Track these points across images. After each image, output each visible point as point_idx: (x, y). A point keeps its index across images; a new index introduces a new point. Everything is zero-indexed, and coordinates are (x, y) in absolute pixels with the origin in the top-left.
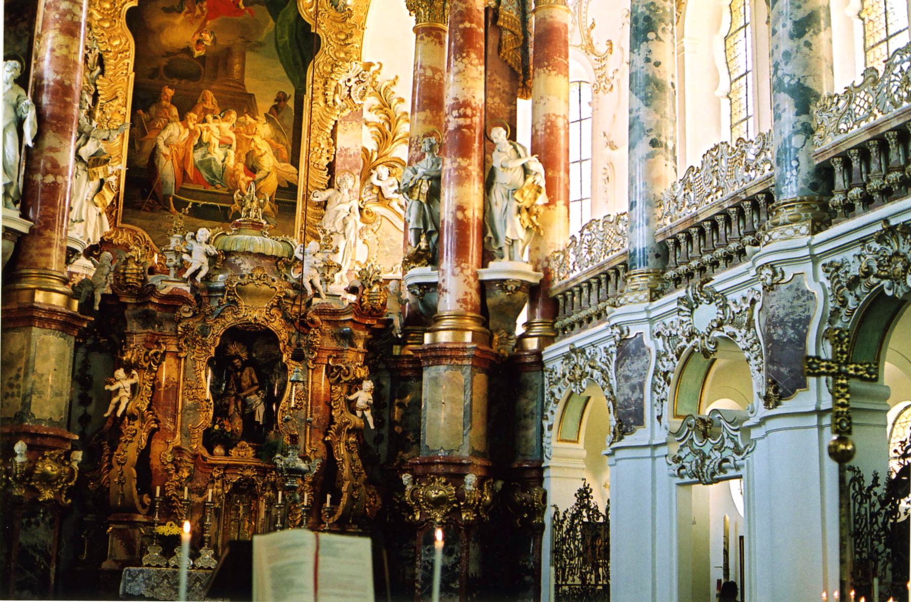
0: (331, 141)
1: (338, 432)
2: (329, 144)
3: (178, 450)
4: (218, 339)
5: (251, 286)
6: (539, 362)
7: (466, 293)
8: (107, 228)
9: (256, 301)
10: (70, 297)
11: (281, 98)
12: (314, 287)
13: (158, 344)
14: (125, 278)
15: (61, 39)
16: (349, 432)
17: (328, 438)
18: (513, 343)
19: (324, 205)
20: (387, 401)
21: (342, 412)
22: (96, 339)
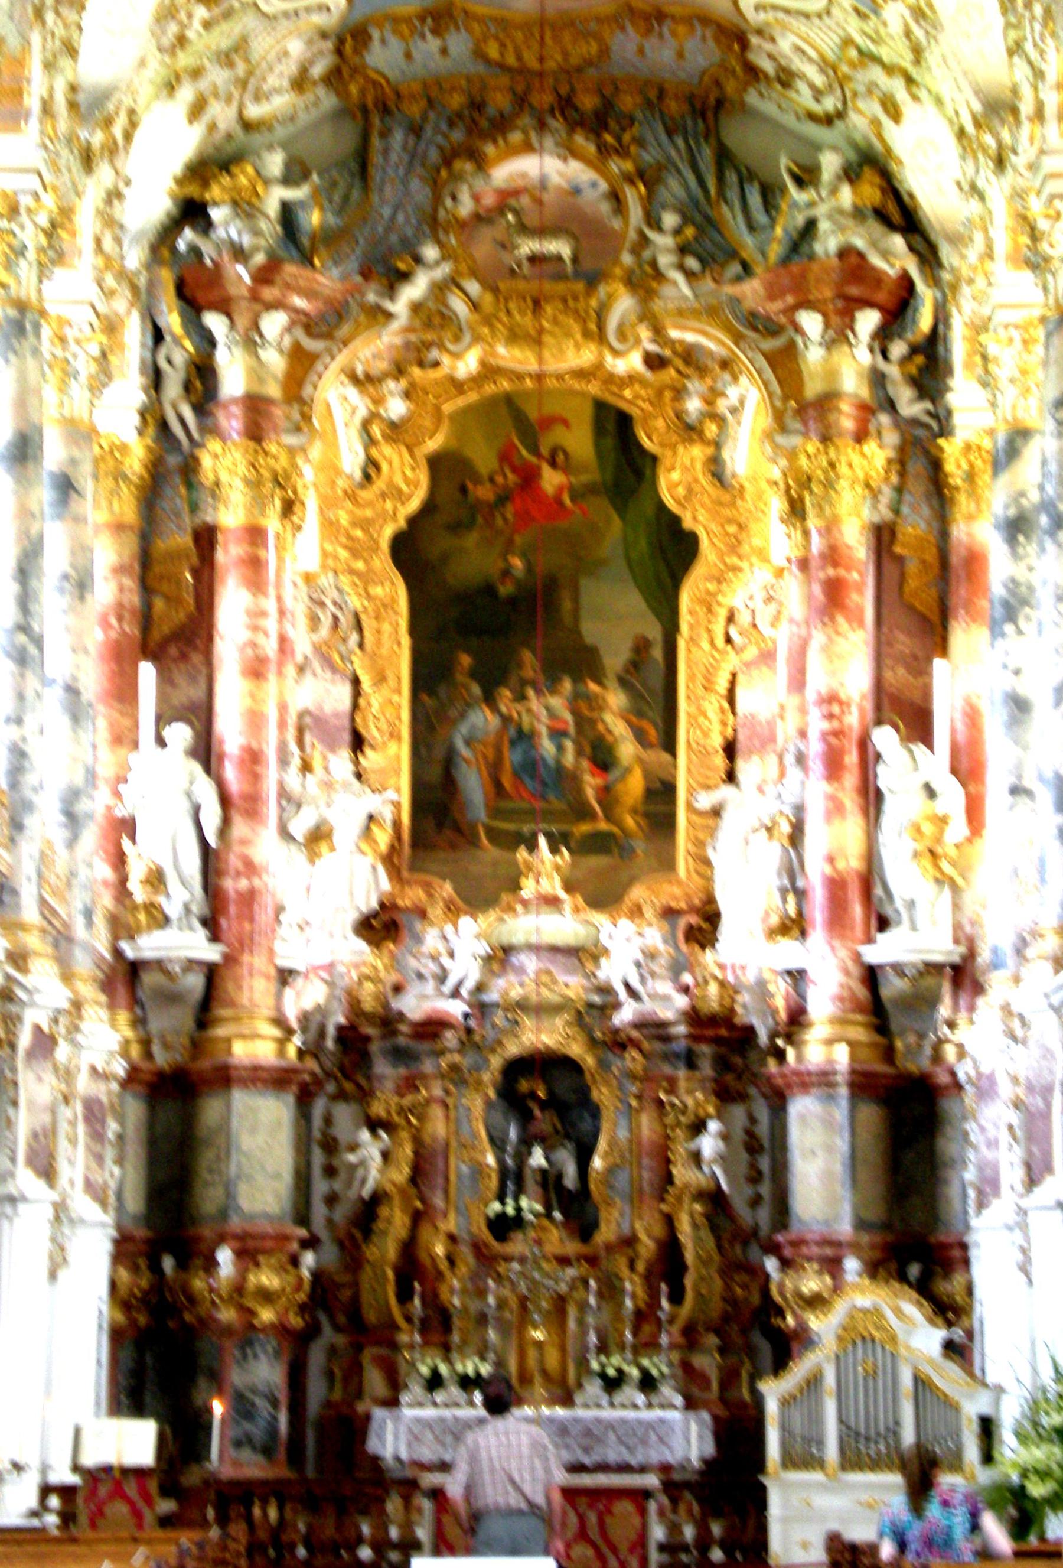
0: (726, 706)
1: (679, 1199)
2: (722, 710)
6: (958, 1086)
7: (842, 986)
8: (385, 885)
10: (282, 1043)
11: (641, 647)
15: (245, 685)
17: (664, 1207)
18: (928, 1051)
19: (716, 812)
20: (766, 1143)
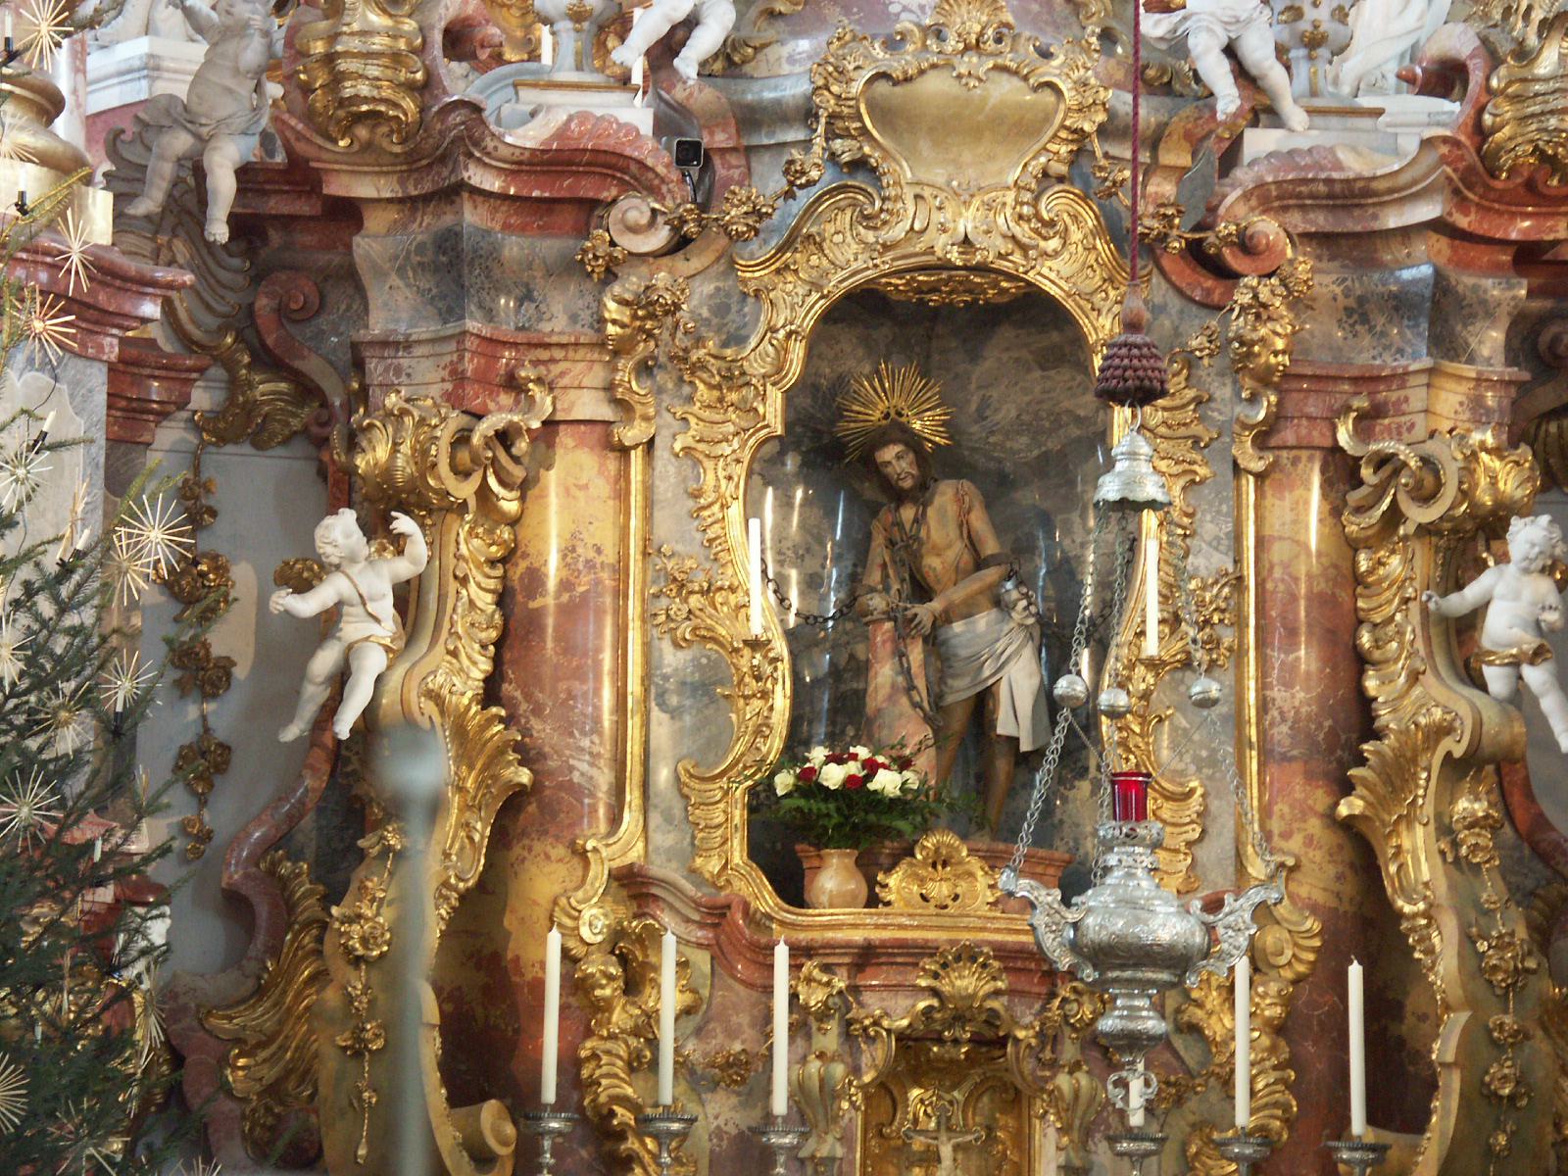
1: (1398, 776)
3: (632, 884)
4: (798, 351)
5: (936, 86)
9: (967, 156)
12: (1243, 75)
13: (513, 384)
14: (337, 79)
16: (1457, 770)
21: (1414, 677)
22: (234, 385)
